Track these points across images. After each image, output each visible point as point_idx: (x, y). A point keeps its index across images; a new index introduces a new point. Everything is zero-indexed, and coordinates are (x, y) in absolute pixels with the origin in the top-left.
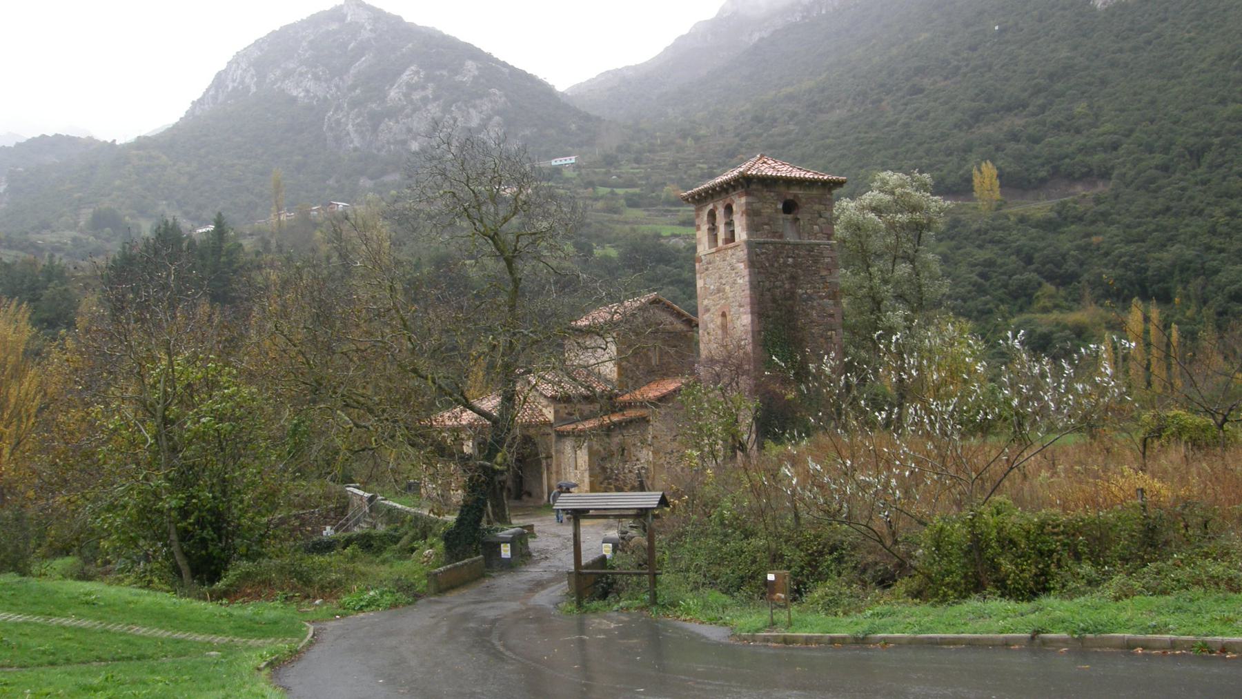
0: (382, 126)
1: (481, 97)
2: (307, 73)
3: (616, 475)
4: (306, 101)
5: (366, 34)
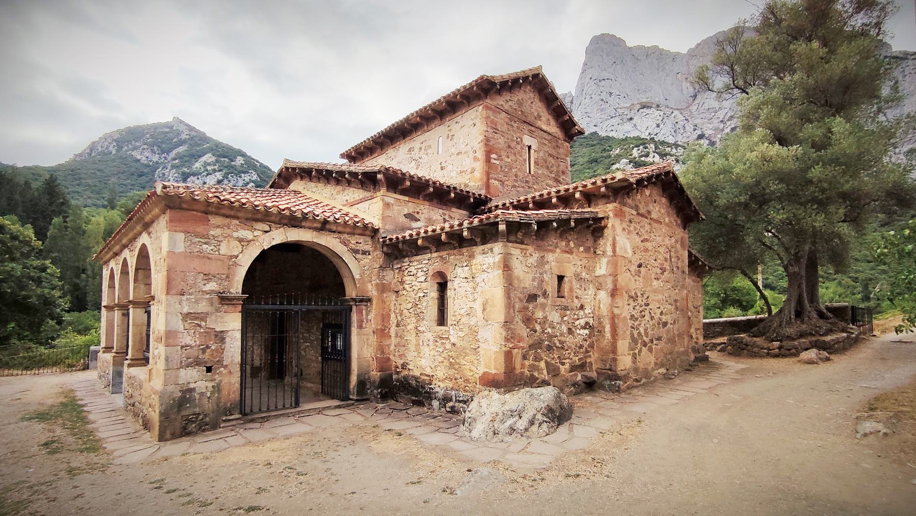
0: (189, 180)
1: (244, 173)
2: (147, 149)
3: (551, 337)
4: (146, 162)
5: (184, 137)
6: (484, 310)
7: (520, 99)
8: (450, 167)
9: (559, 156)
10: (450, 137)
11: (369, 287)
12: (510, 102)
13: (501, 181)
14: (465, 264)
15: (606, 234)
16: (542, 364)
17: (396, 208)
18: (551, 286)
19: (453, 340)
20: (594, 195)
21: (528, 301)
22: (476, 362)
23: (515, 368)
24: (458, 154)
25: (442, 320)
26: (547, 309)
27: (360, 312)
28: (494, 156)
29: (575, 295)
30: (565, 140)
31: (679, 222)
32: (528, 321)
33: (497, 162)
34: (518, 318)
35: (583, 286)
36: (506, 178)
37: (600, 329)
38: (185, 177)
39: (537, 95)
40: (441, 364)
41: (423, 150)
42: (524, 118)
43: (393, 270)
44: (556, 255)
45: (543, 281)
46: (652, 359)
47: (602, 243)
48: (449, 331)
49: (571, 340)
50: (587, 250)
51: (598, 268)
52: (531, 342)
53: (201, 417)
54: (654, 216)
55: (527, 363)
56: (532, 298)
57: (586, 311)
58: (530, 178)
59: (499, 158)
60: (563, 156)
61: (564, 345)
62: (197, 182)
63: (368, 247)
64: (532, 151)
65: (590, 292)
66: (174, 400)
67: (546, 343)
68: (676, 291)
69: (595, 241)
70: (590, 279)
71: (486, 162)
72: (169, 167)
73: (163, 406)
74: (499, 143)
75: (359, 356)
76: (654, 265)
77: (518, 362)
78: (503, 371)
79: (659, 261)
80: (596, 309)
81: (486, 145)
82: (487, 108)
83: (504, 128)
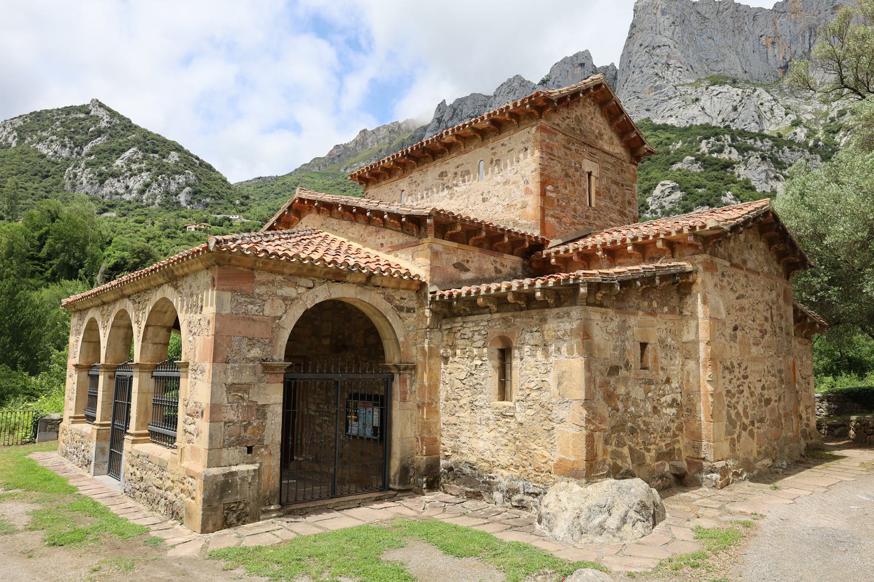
0: (107, 182)
1: (179, 173)
2: (56, 140)
3: (635, 417)
5: (103, 124)
6: (559, 384)
7: (579, 114)
8: (494, 200)
9: (624, 183)
10: (494, 161)
11: (414, 351)
12: (568, 120)
13: (557, 218)
14: (535, 329)
15: (694, 292)
16: (626, 451)
17: (445, 256)
18: (634, 357)
19: (519, 419)
20: (679, 243)
21: (610, 374)
22: (549, 446)
23: (597, 455)
24: (505, 183)
25: (503, 392)
26: (629, 383)
27: (404, 382)
28: (549, 188)
29: (660, 366)
30: (631, 163)
31: (781, 270)
32: (610, 397)
33: (553, 195)
34: (599, 395)
35: (669, 354)
36: (564, 215)
37: (689, 407)
38: (102, 179)
39: (598, 109)
40: (504, 448)
41: (459, 175)
42: (583, 139)
43: (440, 330)
44: (639, 318)
45: (624, 351)
46: (754, 446)
47: (690, 302)
48: (514, 408)
49: (657, 422)
50: (672, 311)
51: (685, 333)
52: (613, 423)
53: (242, 506)
54: (750, 265)
55: (610, 449)
56: (614, 370)
57: (673, 385)
58: (591, 213)
59: (556, 189)
60: (628, 183)
61: (650, 426)
62: (117, 185)
63: (413, 304)
64: (593, 179)
65: (677, 362)
66: (217, 484)
67: (629, 424)
68: (780, 359)
69: (681, 299)
70: (676, 346)
71: (541, 195)
72: (83, 165)
73: (207, 493)
74: (555, 172)
75: (402, 435)
76: (751, 327)
77: (600, 447)
78: (584, 458)
79: (758, 322)
80: (684, 382)
81: (541, 175)
82: (542, 129)
83: (561, 152)
